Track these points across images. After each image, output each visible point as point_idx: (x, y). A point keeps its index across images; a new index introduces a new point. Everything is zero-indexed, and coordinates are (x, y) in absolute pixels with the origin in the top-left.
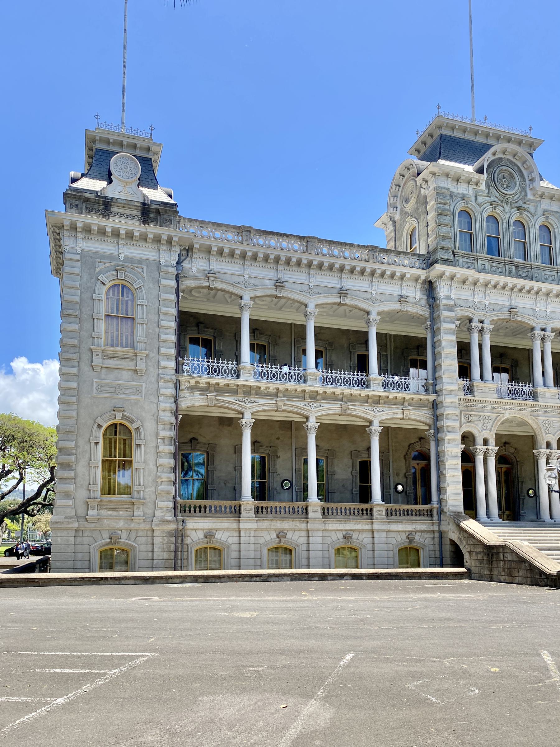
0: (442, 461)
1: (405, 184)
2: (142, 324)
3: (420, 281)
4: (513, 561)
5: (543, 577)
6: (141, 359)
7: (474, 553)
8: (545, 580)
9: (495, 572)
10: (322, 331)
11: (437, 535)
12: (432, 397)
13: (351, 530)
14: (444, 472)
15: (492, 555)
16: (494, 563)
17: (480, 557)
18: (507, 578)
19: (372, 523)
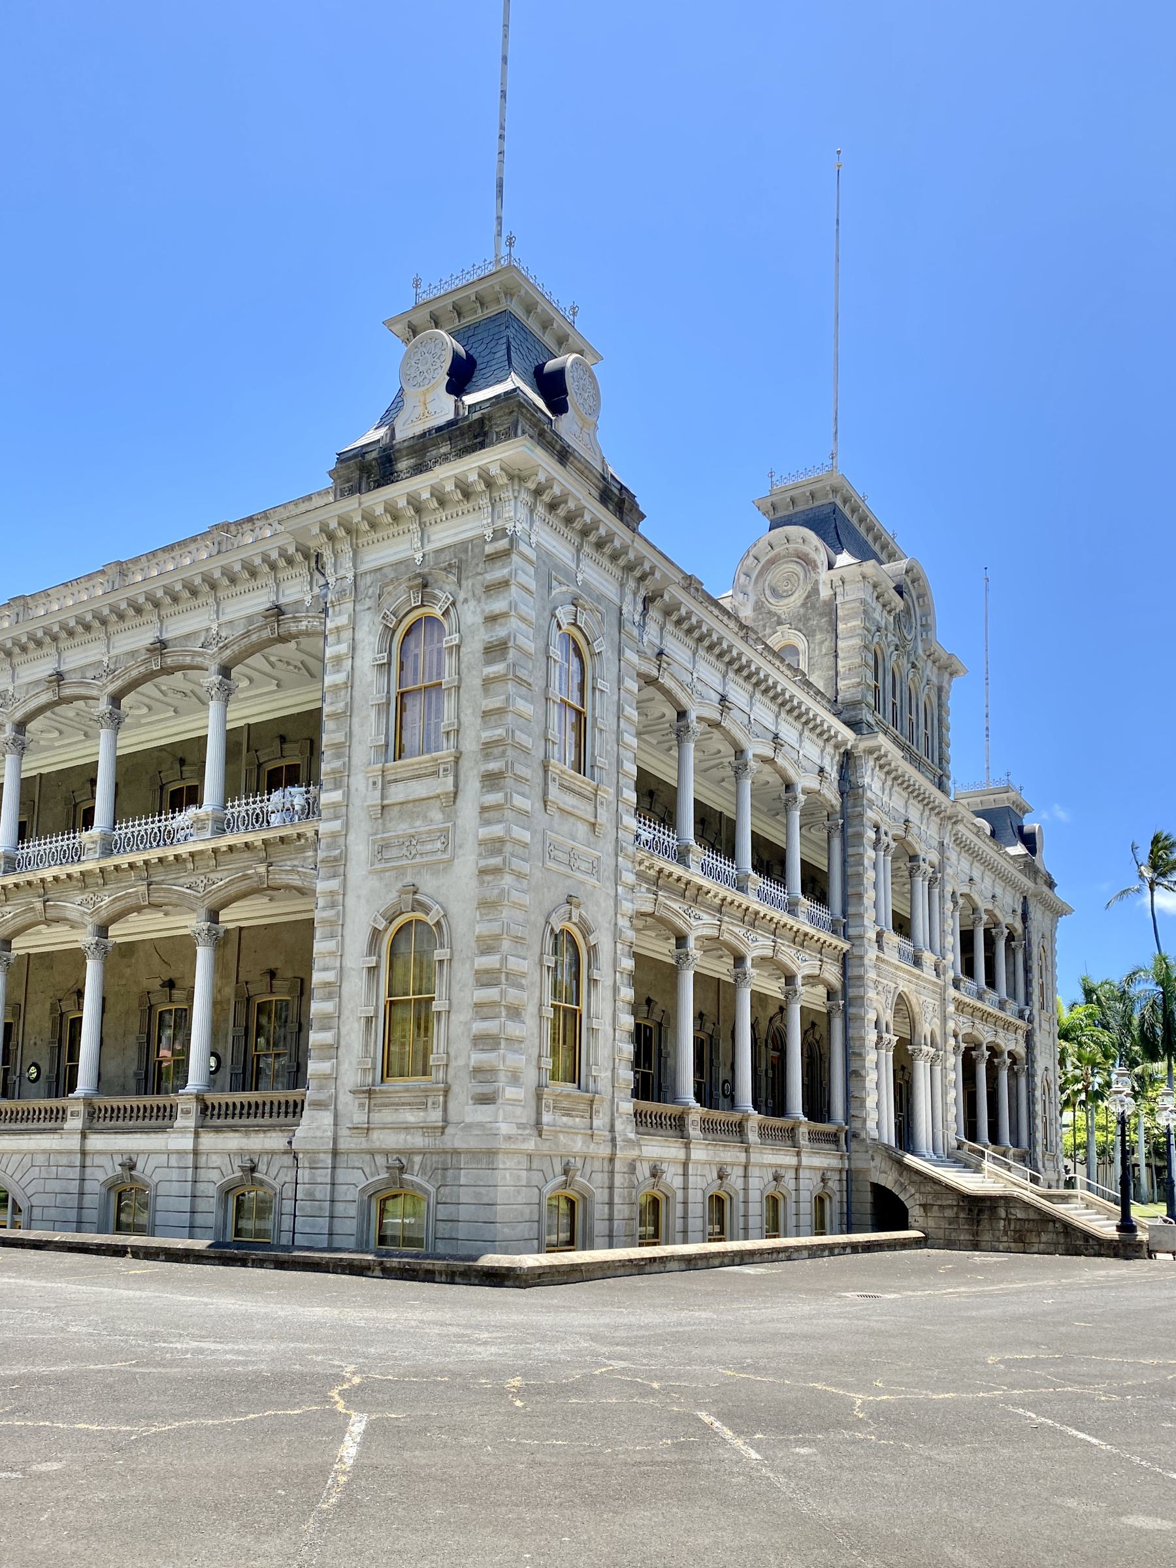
0: (860, 1055)
1: (772, 562)
2: (601, 730)
3: (842, 750)
4: (1029, 1220)
5: (1091, 1242)
6: (602, 803)
7: (936, 1208)
8: (1096, 1247)
9: (987, 1237)
10: (661, 787)
11: (844, 1174)
12: (846, 946)
13: (780, 1166)
14: (863, 1073)
15: (980, 1211)
16: (985, 1224)
17: (949, 1213)
18: (1012, 1245)
19: (798, 1154)
